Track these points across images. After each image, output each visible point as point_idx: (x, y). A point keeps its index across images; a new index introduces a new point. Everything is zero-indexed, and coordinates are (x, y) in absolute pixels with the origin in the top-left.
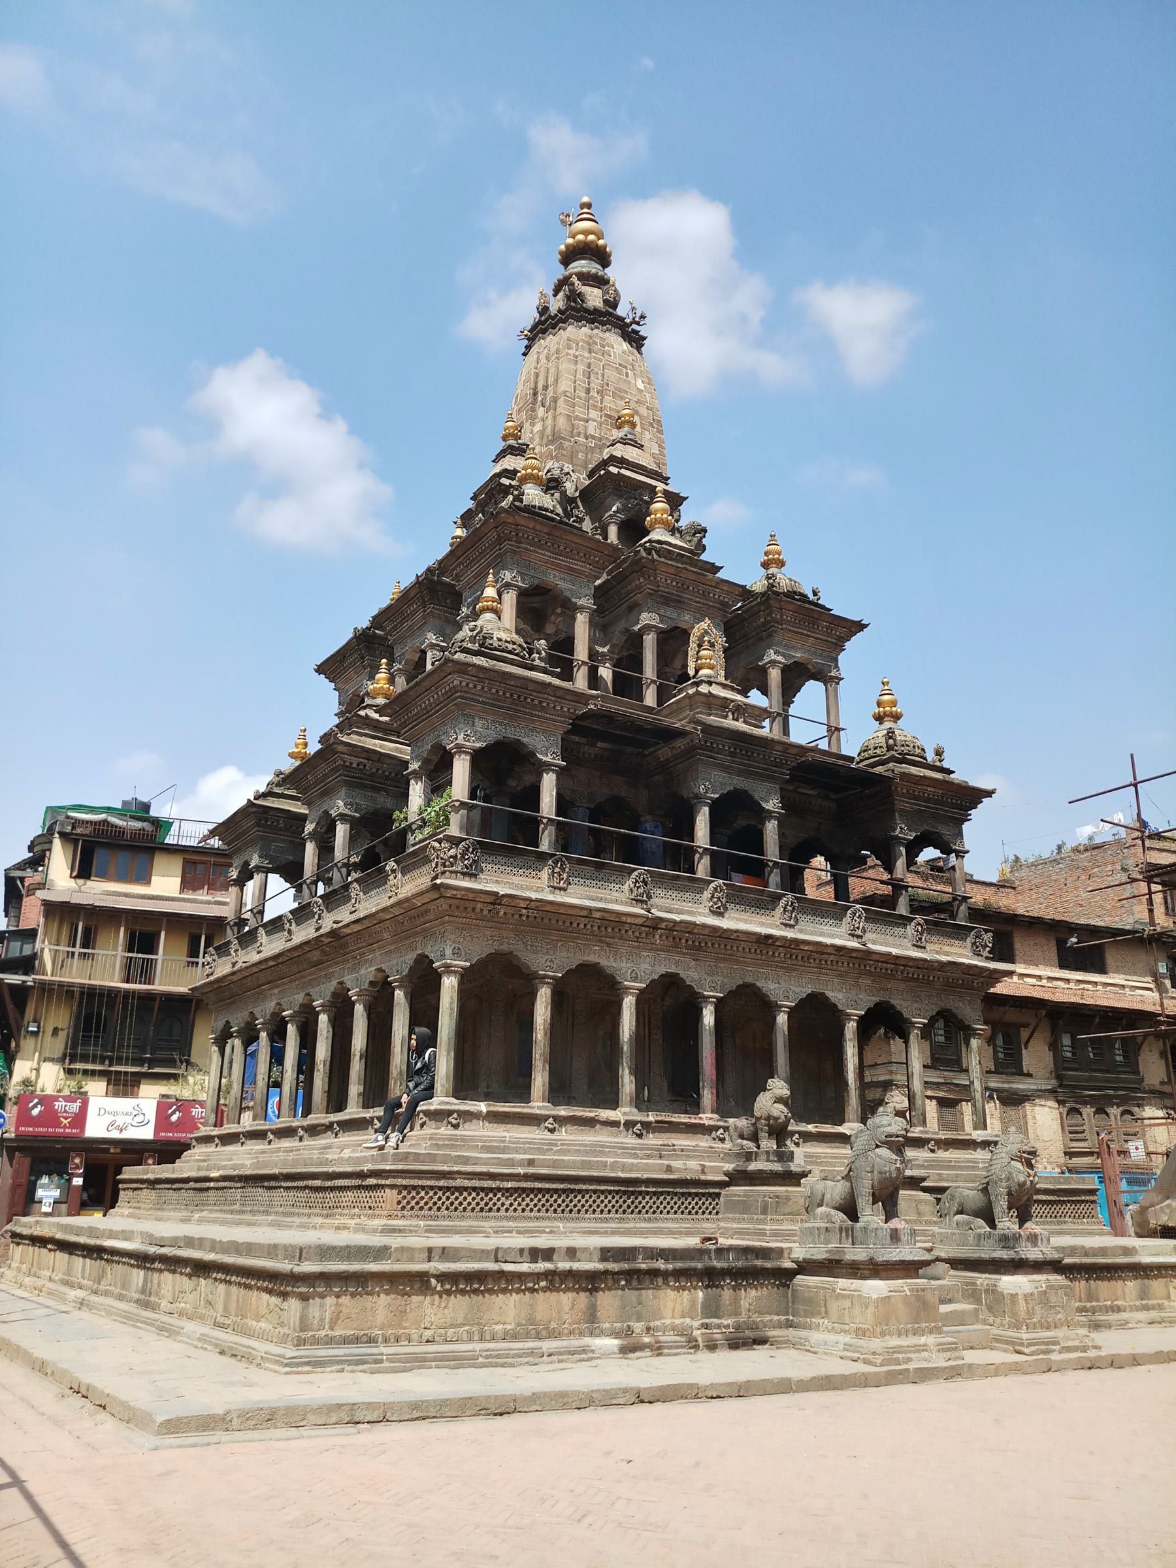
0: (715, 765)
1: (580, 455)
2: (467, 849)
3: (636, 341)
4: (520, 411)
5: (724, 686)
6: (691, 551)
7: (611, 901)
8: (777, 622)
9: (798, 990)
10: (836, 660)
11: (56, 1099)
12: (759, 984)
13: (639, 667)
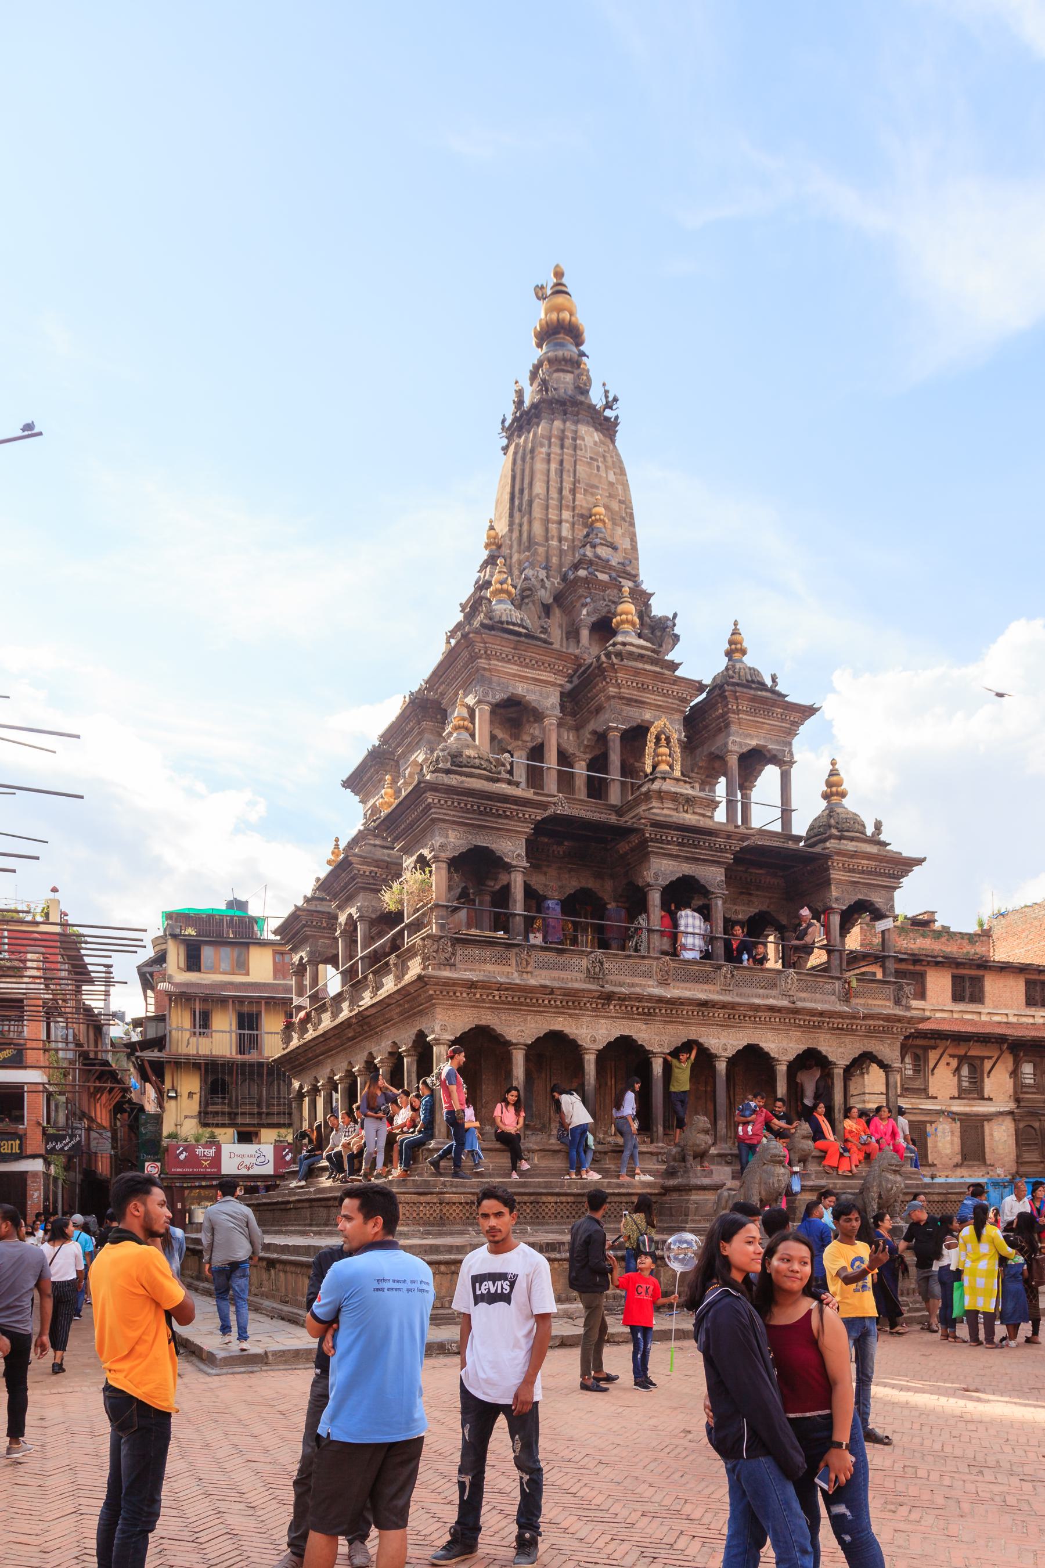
0: (665, 855)
1: (555, 560)
6: (653, 651)
8: (734, 713)
9: (735, 1043)
10: (790, 744)
12: (701, 1040)
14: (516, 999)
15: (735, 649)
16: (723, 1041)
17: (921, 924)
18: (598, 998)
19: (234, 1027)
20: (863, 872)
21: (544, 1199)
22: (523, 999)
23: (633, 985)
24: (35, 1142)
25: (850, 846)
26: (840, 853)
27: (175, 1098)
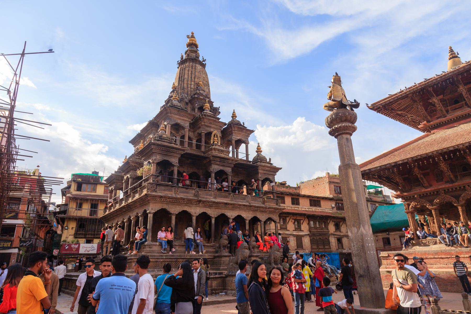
1: (189, 93)
3: (204, 66)
10: (248, 139)
15: (234, 116)
16: (231, 214)
17: (283, 184)
19: (89, 208)
21: (179, 260)
22: (176, 201)
24: (16, 243)
25: (263, 164)
26: (261, 166)
27: (67, 229)
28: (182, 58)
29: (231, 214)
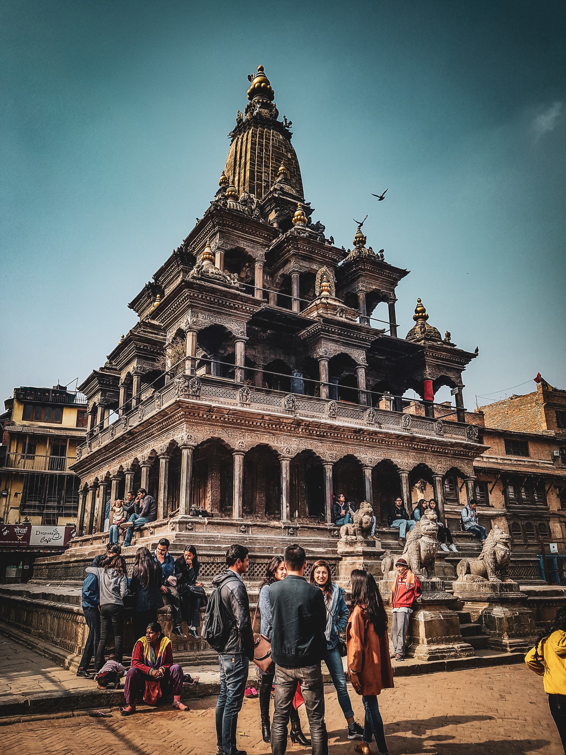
0: (330, 340)
2: (194, 383)
3: (288, 136)
4: (228, 171)
5: (335, 300)
7: (275, 411)
9: (376, 458)
10: (393, 291)
11: (15, 527)
13: (290, 292)
14: (239, 421)
18: (292, 424)
20: (442, 359)
23: (313, 417)
28: (240, 121)
29: (369, 457)
